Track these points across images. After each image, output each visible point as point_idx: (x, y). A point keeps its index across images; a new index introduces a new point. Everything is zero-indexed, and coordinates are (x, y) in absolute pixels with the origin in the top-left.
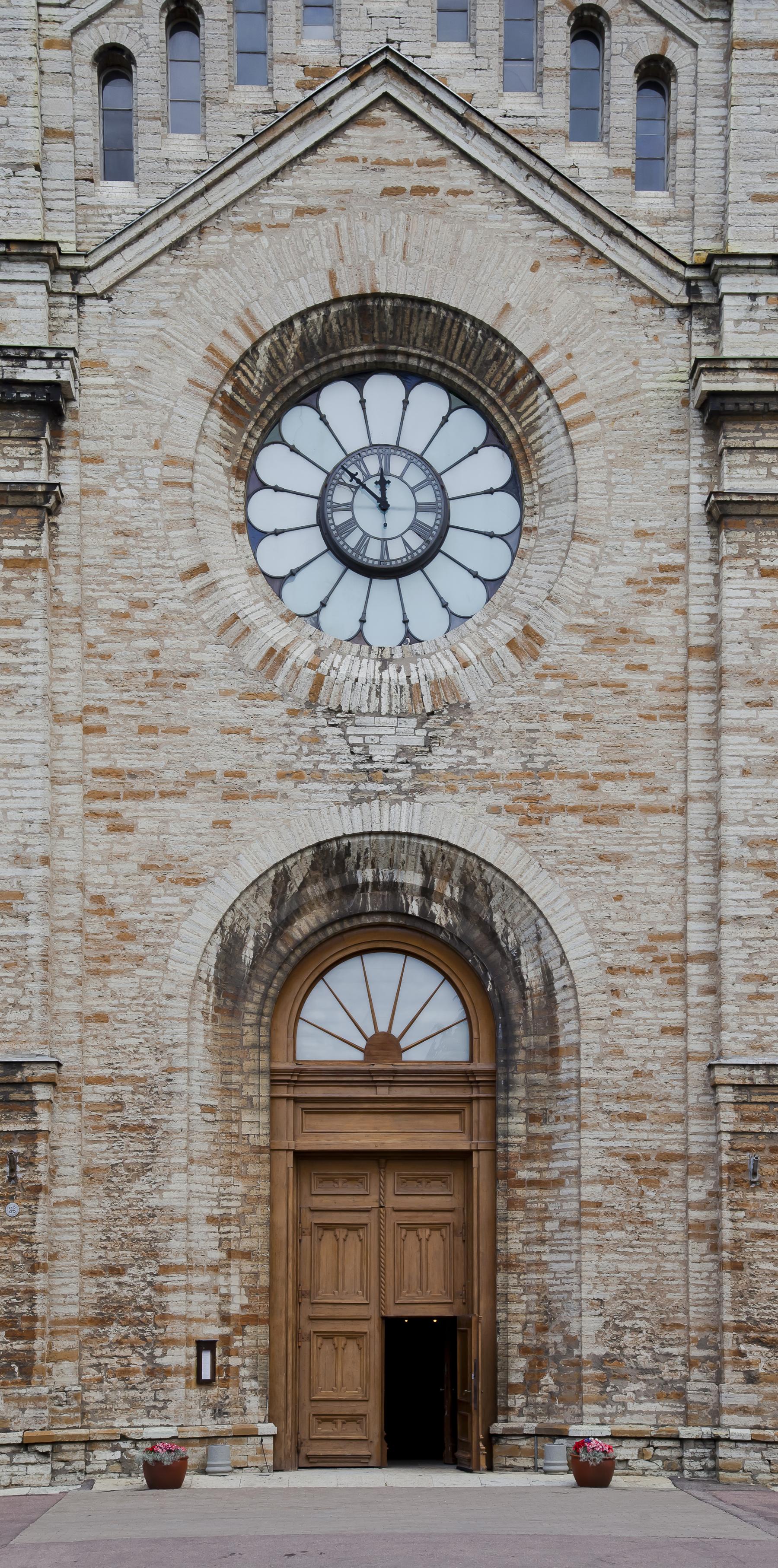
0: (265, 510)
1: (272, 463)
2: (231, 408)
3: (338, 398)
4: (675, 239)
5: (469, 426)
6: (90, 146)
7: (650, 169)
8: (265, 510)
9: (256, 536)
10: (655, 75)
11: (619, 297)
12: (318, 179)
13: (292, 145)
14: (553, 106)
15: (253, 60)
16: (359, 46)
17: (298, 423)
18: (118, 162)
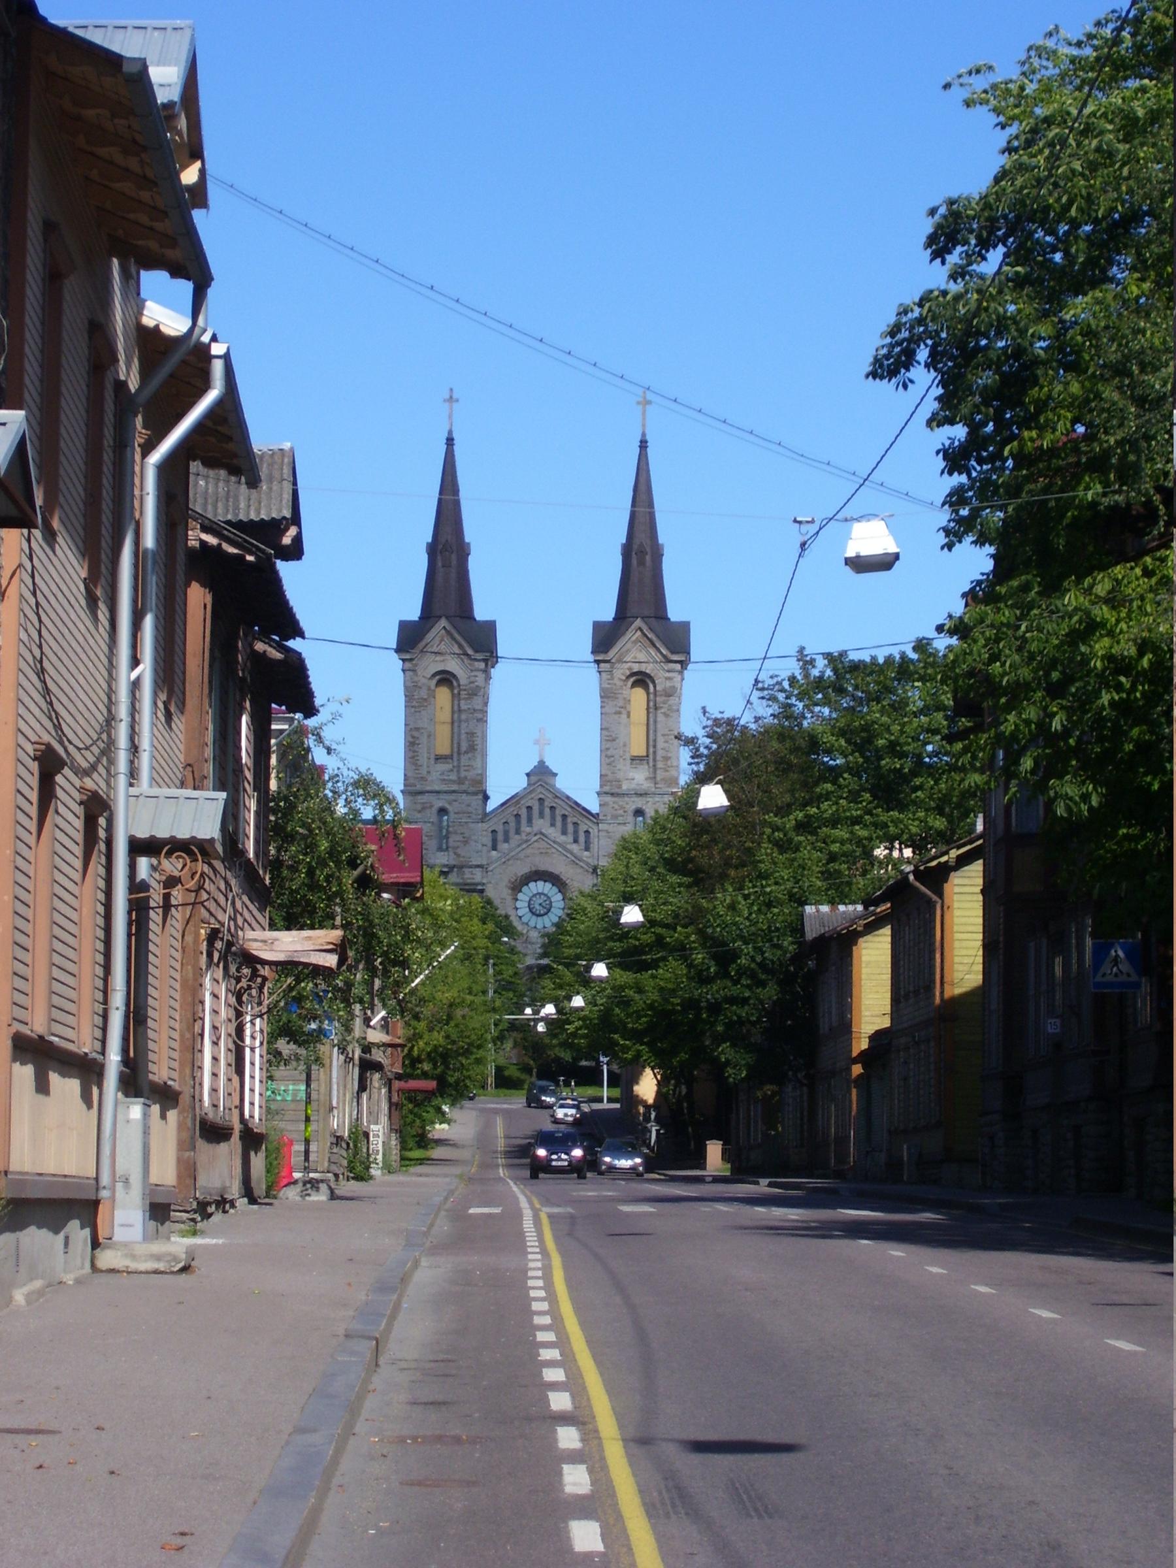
0: (519, 904)
1: (520, 896)
2: (513, 889)
3: (532, 885)
4: (590, 861)
5: (555, 889)
6: (490, 844)
7: (587, 849)
8: (519, 904)
9: (517, 909)
10: (587, 832)
11: (580, 870)
12: (529, 851)
13: (524, 846)
14: (570, 838)
15: (518, 832)
16: (535, 829)
17: (525, 889)
18: (494, 848)
